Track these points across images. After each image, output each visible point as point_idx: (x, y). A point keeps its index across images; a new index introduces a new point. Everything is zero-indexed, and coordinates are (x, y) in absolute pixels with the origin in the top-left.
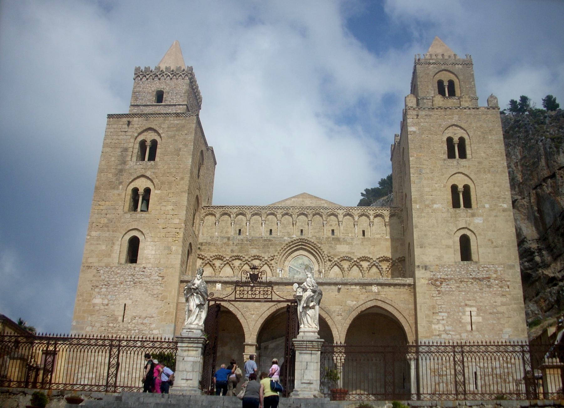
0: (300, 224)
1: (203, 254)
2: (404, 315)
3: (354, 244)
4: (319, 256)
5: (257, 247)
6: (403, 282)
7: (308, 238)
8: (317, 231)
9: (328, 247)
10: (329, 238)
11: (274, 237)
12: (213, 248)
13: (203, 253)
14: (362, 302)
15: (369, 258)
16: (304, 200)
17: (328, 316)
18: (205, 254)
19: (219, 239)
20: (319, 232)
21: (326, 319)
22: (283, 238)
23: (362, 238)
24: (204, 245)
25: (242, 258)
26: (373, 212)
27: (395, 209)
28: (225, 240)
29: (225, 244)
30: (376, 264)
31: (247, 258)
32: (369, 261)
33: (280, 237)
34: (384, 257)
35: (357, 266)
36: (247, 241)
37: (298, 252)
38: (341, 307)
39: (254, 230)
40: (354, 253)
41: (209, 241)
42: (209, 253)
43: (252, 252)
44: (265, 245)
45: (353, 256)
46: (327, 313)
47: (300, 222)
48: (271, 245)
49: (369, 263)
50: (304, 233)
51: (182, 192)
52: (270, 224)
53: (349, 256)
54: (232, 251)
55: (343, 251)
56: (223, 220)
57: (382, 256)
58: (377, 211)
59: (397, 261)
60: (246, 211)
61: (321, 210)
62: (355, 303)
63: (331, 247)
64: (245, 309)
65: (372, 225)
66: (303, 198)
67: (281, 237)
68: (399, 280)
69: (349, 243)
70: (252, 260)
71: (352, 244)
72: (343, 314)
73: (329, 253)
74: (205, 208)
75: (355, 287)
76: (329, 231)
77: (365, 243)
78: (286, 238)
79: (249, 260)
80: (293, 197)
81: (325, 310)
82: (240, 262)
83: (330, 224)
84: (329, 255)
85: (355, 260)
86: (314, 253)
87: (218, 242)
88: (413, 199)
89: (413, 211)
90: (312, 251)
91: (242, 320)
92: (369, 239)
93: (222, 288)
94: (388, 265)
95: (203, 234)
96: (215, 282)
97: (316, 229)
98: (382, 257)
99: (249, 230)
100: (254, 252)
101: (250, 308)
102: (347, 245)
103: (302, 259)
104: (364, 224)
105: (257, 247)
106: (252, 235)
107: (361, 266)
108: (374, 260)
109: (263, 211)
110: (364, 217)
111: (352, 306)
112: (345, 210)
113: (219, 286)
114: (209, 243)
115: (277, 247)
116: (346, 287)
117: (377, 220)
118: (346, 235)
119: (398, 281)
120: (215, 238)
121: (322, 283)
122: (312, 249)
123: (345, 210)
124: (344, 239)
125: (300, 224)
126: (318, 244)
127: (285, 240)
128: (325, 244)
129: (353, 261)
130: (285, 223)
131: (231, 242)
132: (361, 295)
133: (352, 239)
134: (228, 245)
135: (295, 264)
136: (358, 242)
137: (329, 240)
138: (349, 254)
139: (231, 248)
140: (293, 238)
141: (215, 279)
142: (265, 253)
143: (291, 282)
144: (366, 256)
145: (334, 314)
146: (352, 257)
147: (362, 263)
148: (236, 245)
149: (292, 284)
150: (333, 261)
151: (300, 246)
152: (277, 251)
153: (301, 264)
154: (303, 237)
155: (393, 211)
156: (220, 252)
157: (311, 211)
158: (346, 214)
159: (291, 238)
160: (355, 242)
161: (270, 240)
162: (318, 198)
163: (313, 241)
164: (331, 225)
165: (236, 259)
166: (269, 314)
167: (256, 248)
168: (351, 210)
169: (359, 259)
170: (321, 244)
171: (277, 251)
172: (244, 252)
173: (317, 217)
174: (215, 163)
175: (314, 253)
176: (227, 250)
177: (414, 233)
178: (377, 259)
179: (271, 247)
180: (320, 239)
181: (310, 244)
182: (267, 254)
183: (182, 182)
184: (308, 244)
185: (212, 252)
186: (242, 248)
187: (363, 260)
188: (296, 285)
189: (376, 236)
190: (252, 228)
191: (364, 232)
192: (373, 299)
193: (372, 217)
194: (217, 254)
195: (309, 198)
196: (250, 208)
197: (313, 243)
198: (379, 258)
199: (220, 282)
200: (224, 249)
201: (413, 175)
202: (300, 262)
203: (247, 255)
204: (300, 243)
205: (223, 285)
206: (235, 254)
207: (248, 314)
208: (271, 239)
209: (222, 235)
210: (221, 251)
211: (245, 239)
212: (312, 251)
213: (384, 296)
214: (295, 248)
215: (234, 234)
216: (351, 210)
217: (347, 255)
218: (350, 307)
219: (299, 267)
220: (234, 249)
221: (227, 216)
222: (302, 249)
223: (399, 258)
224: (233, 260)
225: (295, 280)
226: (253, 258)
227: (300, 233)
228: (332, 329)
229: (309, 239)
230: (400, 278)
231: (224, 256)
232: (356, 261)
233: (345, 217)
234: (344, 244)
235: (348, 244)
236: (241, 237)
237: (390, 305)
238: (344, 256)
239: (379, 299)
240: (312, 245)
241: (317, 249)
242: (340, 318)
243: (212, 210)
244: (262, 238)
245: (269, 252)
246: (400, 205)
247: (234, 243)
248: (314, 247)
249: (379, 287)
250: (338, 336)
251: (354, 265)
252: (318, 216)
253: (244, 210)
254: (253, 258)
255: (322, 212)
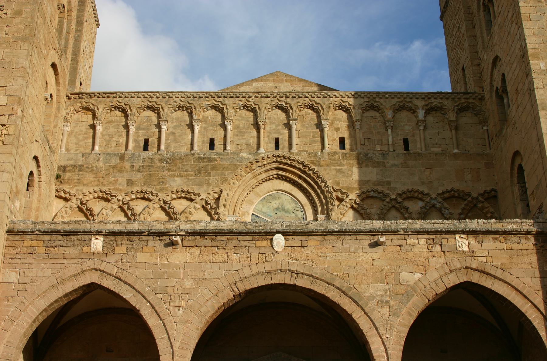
0: (274, 127)
1: (67, 190)
2: (535, 303)
3: (388, 165)
4: (315, 191)
5: (183, 174)
6: (525, 228)
7: (292, 154)
8: (308, 140)
9: (334, 172)
10: (335, 153)
11: (218, 154)
12: (89, 177)
13: (66, 188)
14: (436, 275)
15: (422, 193)
16: (278, 85)
17: (360, 309)
18: (72, 188)
19: (103, 157)
20: (312, 142)
21: (354, 316)
22: (238, 154)
23: (404, 153)
24: (70, 171)
25: (150, 196)
26: (423, 103)
27: (468, 96)
28: (115, 161)
29: (114, 167)
30: (438, 205)
31: (161, 195)
32: (421, 200)
33: (231, 153)
34: (452, 190)
35: (398, 210)
36: (161, 161)
37: (269, 183)
38: (387, 287)
39: (176, 141)
40: (389, 183)
41: (80, 163)
42: (80, 188)
43: (173, 184)
44: (199, 170)
45: (388, 189)
46: (355, 301)
47: (271, 123)
48: (213, 169)
49: (420, 204)
50: (281, 147)
51: (16, 40)
52: (211, 128)
53: (380, 188)
54: (130, 182)
55: (366, 179)
56: (110, 122)
57: (449, 188)
58: (433, 100)
59: (480, 198)
60: (158, 101)
61: (317, 100)
62: (418, 276)
63: (340, 171)
64: (160, 296)
65: (422, 128)
66: (274, 81)
67: (234, 154)
68: (516, 223)
69: (378, 163)
70: (173, 199)
71: (385, 166)
72: (392, 303)
73: (338, 184)
74: (72, 96)
75: (416, 241)
76: (334, 140)
77: (411, 163)
78: (244, 155)
79: (168, 199)
80: (256, 80)
81: (350, 294)
82: (145, 203)
83: (336, 126)
84: (337, 188)
85: (393, 197)
86: (305, 185)
87: (101, 165)
88: (530, 52)
89: (534, 75)
90: (300, 181)
91: (152, 321)
92: (420, 155)
93: (103, 248)
94: (463, 206)
95: (67, 150)
96: (88, 233)
97: (306, 137)
98: (448, 191)
99: (166, 140)
100: (177, 183)
101: (171, 291)
102: (374, 167)
103: (279, 198)
104: (407, 128)
105: (183, 174)
106: (173, 150)
107: (407, 209)
108: (433, 196)
109: (196, 102)
110: (404, 114)
111: (412, 283)
112: (366, 100)
113: (97, 243)
114: (81, 166)
115: (227, 173)
116: (396, 240)
117: (430, 118)
118: (369, 147)
119: (515, 226)
120: (92, 157)
121: (339, 231)
122: (300, 177)
123: (366, 100)
124: (366, 155)
125: (274, 127)
126: (313, 167)
127: (242, 159)
128: (328, 165)
129: (387, 200)
130: (241, 126)
131: (127, 165)
132: (431, 259)
133: (384, 155)
134: (121, 171)
135: (265, 210)
136: (396, 162)
137: (337, 157)
138: (378, 185)
139: (126, 175)
140: (260, 154)
141: (88, 227)
142: (200, 185)
143: (268, 229)
144: (416, 188)
145: (371, 304)
146: (387, 192)
147: (406, 204)
148: (139, 171)
149: (270, 234)
150: (347, 200)
151: (275, 172)
152: (226, 180)
153: (278, 209)
154: (280, 152)
155: (463, 101)
156: (103, 185)
157: (295, 100)
158: (367, 106)
159: (254, 154)
160: (390, 161)
161: (210, 160)
162: (306, 81)
163: (301, 160)
164: (337, 129)
165: (137, 198)
166: (217, 306)
167: (180, 176)
168: (377, 100)
169: (400, 195)
170: (320, 166)
171: (226, 180)
172: (155, 183)
173: (307, 113)
174: (98, 25)
175: (305, 185)
176: (120, 180)
177: (542, 120)
178: (439, 194)
179: (213, 173)
180: (315, 156)
181: (294, 167)
182: (205, 187)
183: (17, 20)
184: (291, 166)
185: (86, 185)
186: (150, 175)
187: (408, 198)
188: (279, 240)
189: (432, 149)
190: (171, 137)
191: (406, 142)
192: (458, 266)
193: (421, 114)
194: (97, 189)
195: (286, 82)
196: (167, 96)
197: (302, 163)
198: (443, 193)
199: (99, 233)
200: (111, 179)
201: (525, 4)
202: (275, 204)
203: (161, 190)
204: (274, 165)
205: (107, 241)
206: (136, 188)
207: (164, 306)
208: (213, 156)
209: (109, 151)
210: (105, 182)
211: (158, 157)
212: (300, 181)
213: (484, 259)
214: (264, 176)
215: (136, 147)
216: (377, 100)
217: (376, 188)
218: (408, 285)
219: (273, 214)
220: (134, 178)
221: (119, 114)
222: (279, 177)
223: (485, 192)
224: (132, 200)
225: (276, 227)
226: (174, 196)
227: (273, 145)
228: (369, 340)
229: (293, 157)
230: (518, 220)
231: (113, 192)
232: (395, 199)
233: (367, 114)
234: (367, 166)
235: (377, 165)
236: (149, 154)
237: (500, 279)
238: (369, 188)
239: (474, 266)
240: (299, 169)
241: (309, 176)
242: (386, 311)
243: (87, 100)
244: (193, 154)
245: (209, 184)
246: (477, 90)
247: (133, 166)
248: (304, 172)
249: (472, 241)
250: (384, 354)
251: (391, 208)
252: (310, 111)
253: (155, 100)
254: (174, 196)
255: (318, 104)
